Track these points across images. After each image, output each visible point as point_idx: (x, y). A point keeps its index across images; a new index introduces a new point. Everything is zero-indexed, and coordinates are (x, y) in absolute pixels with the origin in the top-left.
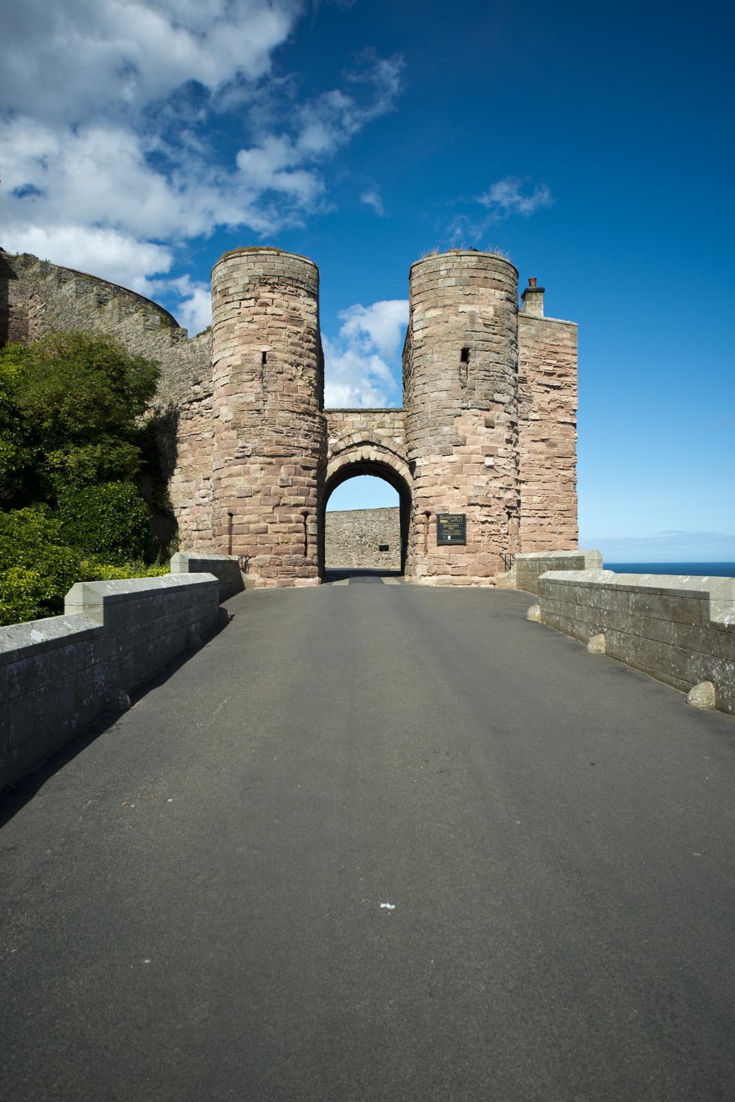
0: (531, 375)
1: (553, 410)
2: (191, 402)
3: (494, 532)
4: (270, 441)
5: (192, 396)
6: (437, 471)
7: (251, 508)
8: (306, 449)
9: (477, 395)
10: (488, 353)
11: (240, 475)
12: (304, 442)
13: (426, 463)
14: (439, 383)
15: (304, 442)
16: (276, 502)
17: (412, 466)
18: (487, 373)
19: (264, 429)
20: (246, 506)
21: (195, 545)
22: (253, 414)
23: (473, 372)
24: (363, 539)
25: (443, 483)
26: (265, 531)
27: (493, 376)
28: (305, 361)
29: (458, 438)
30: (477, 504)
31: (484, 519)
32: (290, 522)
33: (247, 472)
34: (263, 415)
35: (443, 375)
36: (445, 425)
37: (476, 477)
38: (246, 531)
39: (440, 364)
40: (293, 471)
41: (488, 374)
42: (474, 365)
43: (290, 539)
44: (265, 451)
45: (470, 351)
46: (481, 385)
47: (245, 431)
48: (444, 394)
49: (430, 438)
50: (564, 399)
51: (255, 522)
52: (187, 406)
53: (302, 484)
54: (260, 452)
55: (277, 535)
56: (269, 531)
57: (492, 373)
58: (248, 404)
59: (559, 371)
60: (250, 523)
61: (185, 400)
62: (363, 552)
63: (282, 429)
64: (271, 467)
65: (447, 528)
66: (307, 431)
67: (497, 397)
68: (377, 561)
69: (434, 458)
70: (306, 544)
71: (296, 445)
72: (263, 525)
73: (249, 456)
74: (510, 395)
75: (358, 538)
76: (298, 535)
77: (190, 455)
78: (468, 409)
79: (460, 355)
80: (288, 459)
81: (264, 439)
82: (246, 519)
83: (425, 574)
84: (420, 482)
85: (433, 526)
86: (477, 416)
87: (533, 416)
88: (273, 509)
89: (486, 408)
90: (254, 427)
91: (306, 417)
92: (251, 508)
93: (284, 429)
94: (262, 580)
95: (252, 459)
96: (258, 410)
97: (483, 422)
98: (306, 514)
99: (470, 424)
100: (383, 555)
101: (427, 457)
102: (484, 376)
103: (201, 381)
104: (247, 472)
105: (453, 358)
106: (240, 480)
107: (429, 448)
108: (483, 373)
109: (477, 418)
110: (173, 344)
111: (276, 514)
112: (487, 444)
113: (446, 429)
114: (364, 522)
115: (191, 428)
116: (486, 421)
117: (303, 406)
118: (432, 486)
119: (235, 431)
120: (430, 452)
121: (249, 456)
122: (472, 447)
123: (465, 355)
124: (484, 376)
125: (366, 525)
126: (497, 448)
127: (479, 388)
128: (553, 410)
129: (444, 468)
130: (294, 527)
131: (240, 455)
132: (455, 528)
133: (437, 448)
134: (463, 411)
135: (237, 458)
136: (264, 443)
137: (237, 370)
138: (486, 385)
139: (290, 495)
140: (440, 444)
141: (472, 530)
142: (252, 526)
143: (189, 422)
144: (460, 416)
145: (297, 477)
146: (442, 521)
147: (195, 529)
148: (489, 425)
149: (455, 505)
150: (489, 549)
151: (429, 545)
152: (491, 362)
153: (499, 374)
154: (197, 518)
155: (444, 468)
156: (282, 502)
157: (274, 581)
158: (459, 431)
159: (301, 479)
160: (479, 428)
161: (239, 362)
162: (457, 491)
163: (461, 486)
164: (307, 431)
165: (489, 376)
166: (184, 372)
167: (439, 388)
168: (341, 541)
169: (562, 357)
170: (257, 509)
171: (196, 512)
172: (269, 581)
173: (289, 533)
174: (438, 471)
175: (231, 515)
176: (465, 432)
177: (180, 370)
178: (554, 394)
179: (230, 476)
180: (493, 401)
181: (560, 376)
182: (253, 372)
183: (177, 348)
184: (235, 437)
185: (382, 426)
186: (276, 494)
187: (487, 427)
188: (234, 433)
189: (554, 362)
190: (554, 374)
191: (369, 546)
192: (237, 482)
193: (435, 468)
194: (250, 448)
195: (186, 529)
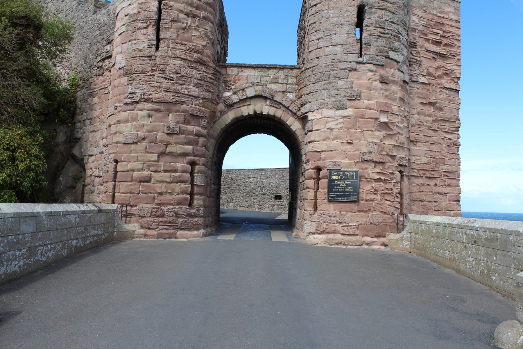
0: (421, 42)
1: (440, 77)
2: (103, 60)
3: (387, 191)
4: (159, 87)
5: (105, 54)
6: (329, 125)
7: (136, 155)
8: (196, 97)
9: (372, 51)
10: (383, 12)
11: (127, 121)
12: (195, 91)
13: (318, 117)
14: (334, 37)
15: (195, 91)
16: (162, 149)
17: (303, 119)
18: (382, 31)
19: (154, 75)
20: (130, 153)
21: (96, 190)
22: (144, 60)
23: (368, 28)
24: (264, 190)
25: (336, 138)
26: (148, 180)
27: (388, 34)
28: (202, 14)
29: (353, 92)
30: (371, 161)
31: (377, 177)
32: (175, 171)
33: (135, 119)
34: (154, 62)
35: (338, 29)
36: (340, 79)
37: (370, 132)
38: (129, 179)
39: (335, 19)
40: (182, 119)
41: (384, 32)
42: (370, 21)
43: (174, 189)
44: (154, 98)
45: (366, 8)
46: (377, 41)
47: (135, 77)
48: (338, 49)
49: (323, 91)
51: (138, 170)
52: (100, 64)
53: (190, 133)
54: (149, 99)
55: (160, 185)
56: (152, 180)
57: (387, 31)
58: (141, 50)
59: (445, 41)
60: (133, 170)
61: (99, 59)
62: (263, 199)
63: (172, 76)
64: (159, 115)
65: (339, 185)
66: (199, 80)
67: (392, 54)
68: (273, 206)
69: (328, 112)
70: (192, 194)
71: (186, 93)
72: (146, 173)
73: (137, 103)
74: (403, 55)
75: (259, 189)
76: (183, 185)
77: (98, 107)
78: (364, 63)
79: (356, 11)
80: (177, 107)
81: (153, 85)
82: (130, 166)
83: (313, 231)
84: (312, 136)
85: (324, 182)
86: (372, 71)
88: (158, 156)
89: (381, 64)
90: (143, 73)
91: (200, 67)
92: (136, 155)
93: (174, 76)
94: (142, 231)
95: (140, 106)
96: (150, 56)
97: (378, 77)
98: (193, 164)
99: (365, 78)
100: (277, 203)
101: (320, 111)
102: (380, 32)
103: (112, 40)
105: (349, 13)
106: (127, 126)
107: (322, 101)
108: (379, 30)
109: (372, 74)
110: (95, 12)
111: (161, 163)
112: (381, 100)
113: (341, 83)
114: (264, 178)
115: (102, 83)
116: (381, 76)
117: (196, 55)
118: (324, 140)
119: (126, 78)
120: (323, 106)
121: (137, 103)
122: (366, 102)
123: (361, 11)
124: (380, 32)
125: (265, 180)
126: (391, 104)
127: (375, 44)
128: (440, 77)
129: (337, 122)
130: (179, 177)
131: (129, 101)
132: (348, 185)
133: (330, 101)
134: (358, 66)
135: (126, 104)
136: (153, 89)
137: (133, 19)
138: (381, 42)
139: (177, 143)
140: (335, 97)
141: (365, 189)
142: (136, 174)
143: (101, 77)
144: (355, 70)
145: (186, 126)
146: (333, 177)
147: (97, 175)
148: (384, 81)
149: (347, 161)
150: (382, 208)
151: (319, 201)
152: (386, 20)
153: (395, 34)
154: (99, 165)
155: (337, 122)
156: (168, 150)
157: (154, 232)
158: (354, 85)
159: (190, 128)
160: (374, 83)
161: (135, 11)
162: (350, 146)
163: (355, 142)
164: (199, 80)
165: (385, 34)
166: (101, 34)
167: (334, 42)
168: (247, 191)
169: (447, 28)
170: (142, 156)
171: (99, 159)
172: (149, 232)
173: (173, 182)
174: (331, 125)
175: (116, 161)
176: (360, 86)
177: (98, 32)
179: (119, 122)
180: (388, 57)
181: (445, 45)
182: (147, 19)
183: (97, 15)
184: (126, 84)
186: (161, 142)
187: (381, 82)
189: (441, 32)
190: (441, 43)
191: (268, 195)
192: (124, 128)
193: (328, 122)
194: (139, 94)
195: (91, 175)
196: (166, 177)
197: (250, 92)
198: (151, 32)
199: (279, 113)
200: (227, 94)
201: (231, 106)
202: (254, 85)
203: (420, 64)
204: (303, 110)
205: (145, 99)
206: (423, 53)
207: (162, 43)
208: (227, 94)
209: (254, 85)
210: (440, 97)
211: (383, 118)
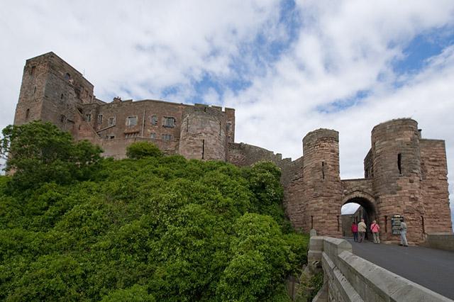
12: (337, 191)
17: (376, 198)
26: (324, 222)
33: (318, 202)
48: (391, 172)
50: (441, 170)
70: (339, 227)
82: (318, 218)
87: (428, 177)
98: (338, 216)
104: (318, 202)
113: (393, 184)
120: (385, 194)
148: (411, 182)
175: (312, 217)
178: (437, 169)
185: (363, 185)
188: (313, 189)
196: (330, 221)
197: (354, 189)
198: (321, 172)
199: (366, 196)
200: (345, 191)
201: (346, 195)
202: (355, 187)
203: (426, 171)
204: (376, 195)
205: (322, 196)
206: (428, 166)
207: (325, 177)
208: (345, 191)
209: (355, 187)
210: (438, 184)
211: (412, 196)
